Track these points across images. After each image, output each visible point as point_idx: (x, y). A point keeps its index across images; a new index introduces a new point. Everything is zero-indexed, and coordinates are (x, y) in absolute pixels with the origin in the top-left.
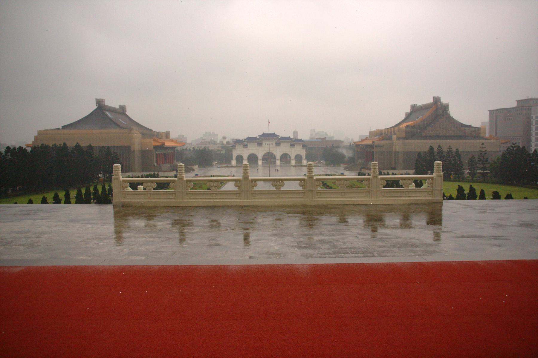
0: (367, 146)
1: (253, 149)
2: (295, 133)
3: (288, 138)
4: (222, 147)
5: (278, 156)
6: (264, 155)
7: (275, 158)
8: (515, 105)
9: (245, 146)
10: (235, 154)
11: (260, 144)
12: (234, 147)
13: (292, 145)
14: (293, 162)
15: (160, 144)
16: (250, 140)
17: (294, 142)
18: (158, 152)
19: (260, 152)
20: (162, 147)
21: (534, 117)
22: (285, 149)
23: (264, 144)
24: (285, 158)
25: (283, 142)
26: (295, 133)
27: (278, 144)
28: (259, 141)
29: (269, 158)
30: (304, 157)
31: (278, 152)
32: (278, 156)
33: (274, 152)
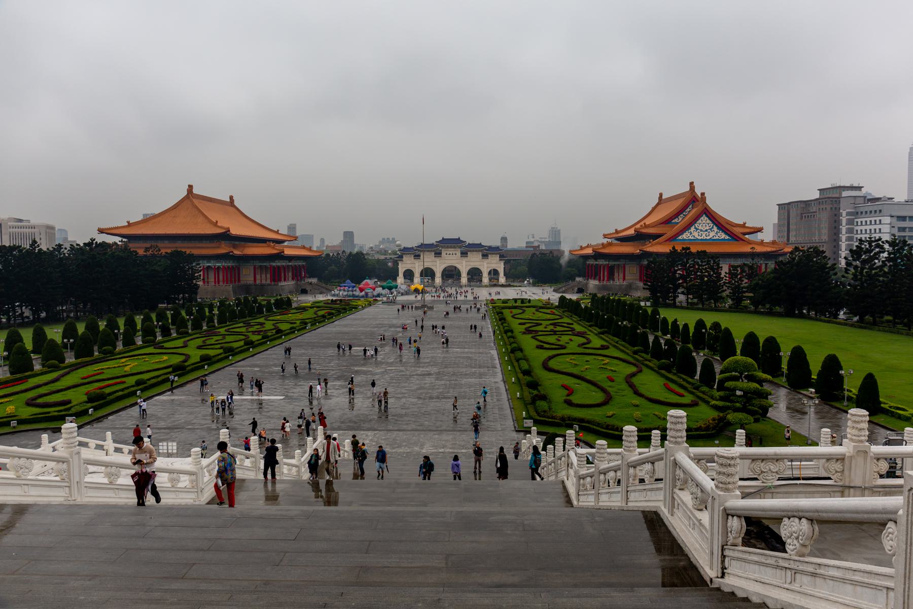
0: (586, 257)
1: (429, 261)
2: (504, 239)
3: (480, 245)
6: (445, 270)
7: (459, 274)
8: (817, 195)
9: (417, 257)
10: (402, 268)
11: (438, 254)
12: (401, 257)
13: (485, 256)
14: (486, 280)
15: (275, 252)
16: (424, 248)
17: (486, 252)
19: (438, 267)
21: (844, 214)
22: (475, 260)
23: (443, 254)
24: (475, 275)
26: (504, 239)
27: (464, 254)
28: (436, 249)
29: (451, 274)
31: (464, 267)
33: (458, 266)
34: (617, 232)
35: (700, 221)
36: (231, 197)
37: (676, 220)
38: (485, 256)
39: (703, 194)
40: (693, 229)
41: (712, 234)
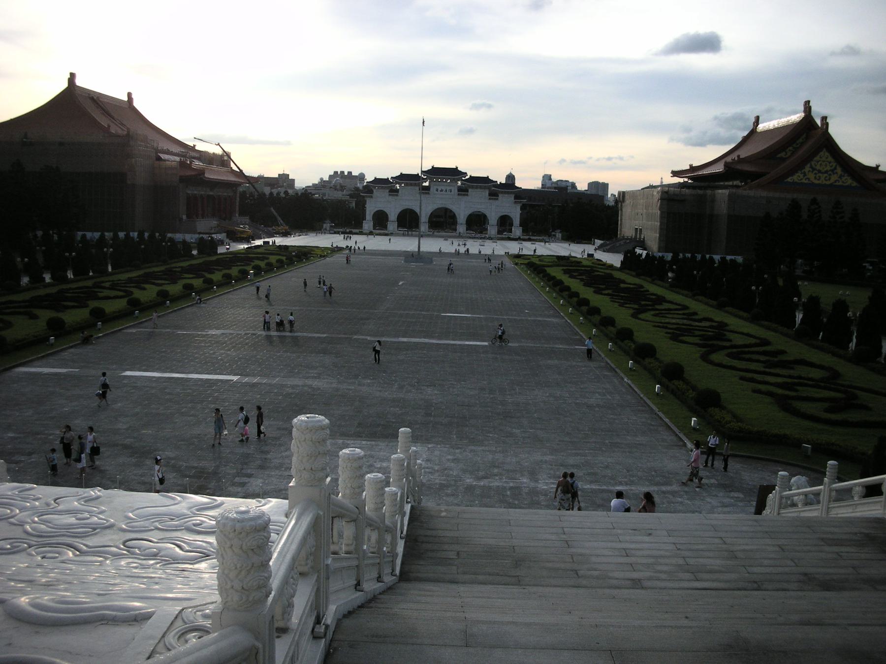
3: (486, 180)
4: (351, 196)
5: (462, 218)
9: (394, 192)
10: (371, 208)
12: (371, 192)
13: (493, 195)
14: (492, 230)
18: (192, 191)
19: (425, 208)
20: (198, 179)
25: (473, 187)
27: (463, 191)
30: (517, 221)
31: (462, 210)
32: (462, 218)
33: (454, 208)
34: (693, 169)
35: (817, 158)
36: (129, 95)
37: (782, 155)
38: (493, 195)
39: (824, 119)
40: (807, 168)
41: (834, 178)
